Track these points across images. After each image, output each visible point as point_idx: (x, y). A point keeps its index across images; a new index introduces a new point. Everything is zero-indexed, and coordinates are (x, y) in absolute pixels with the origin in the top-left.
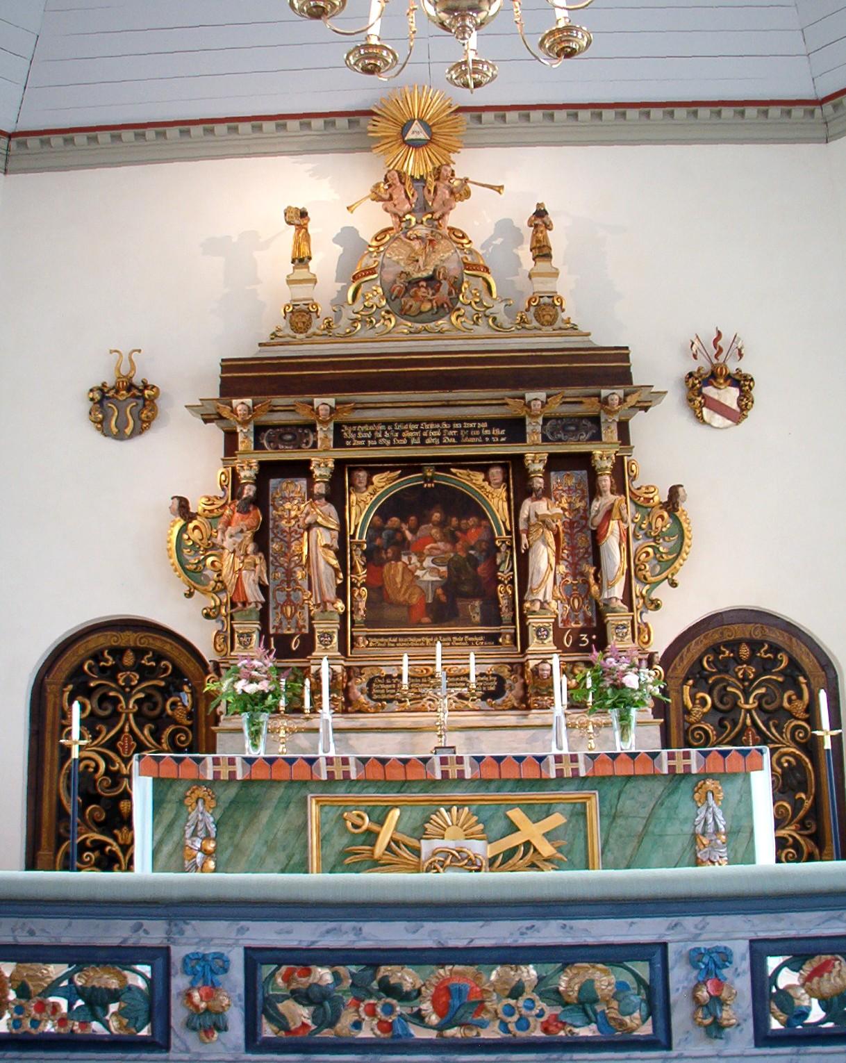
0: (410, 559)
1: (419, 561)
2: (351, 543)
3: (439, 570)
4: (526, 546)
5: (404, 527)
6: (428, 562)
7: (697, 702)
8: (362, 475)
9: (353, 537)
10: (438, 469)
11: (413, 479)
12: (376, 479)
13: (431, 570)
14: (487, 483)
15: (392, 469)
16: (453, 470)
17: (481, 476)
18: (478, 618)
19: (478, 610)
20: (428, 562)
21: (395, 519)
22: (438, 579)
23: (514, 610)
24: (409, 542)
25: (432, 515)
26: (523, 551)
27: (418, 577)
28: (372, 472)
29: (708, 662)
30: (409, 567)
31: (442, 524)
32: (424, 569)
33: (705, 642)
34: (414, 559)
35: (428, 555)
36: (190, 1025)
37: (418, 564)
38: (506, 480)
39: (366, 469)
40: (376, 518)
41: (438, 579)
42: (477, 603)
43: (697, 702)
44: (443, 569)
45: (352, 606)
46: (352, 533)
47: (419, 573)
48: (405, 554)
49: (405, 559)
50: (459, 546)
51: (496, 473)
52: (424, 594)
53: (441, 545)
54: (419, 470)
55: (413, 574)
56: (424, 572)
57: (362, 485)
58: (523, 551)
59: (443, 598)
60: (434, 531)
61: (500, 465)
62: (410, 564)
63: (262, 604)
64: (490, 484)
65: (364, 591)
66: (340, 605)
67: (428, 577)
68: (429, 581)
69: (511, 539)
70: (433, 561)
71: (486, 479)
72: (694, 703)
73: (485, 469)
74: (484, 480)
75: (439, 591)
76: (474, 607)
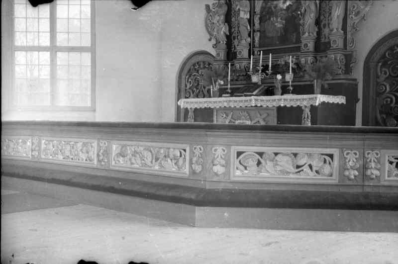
0: (273, 19)
6: (279, 20)
7: (383, 72)
18: (294, 41)
19: (295, 37)
20: (279, 20)
22: (282, 26)
29: (388, 54)
32: (277, 22)
33: (388, 45)
34: (275, 19)
36: (379, 183)
43: (383, 72)
44: (284, 22)
47: (276, 24)
49: (272, 19)
52: (277, 32)
65: (258, 34)
66: (249, 39)
70: (281, 19)
72: (381, 73)
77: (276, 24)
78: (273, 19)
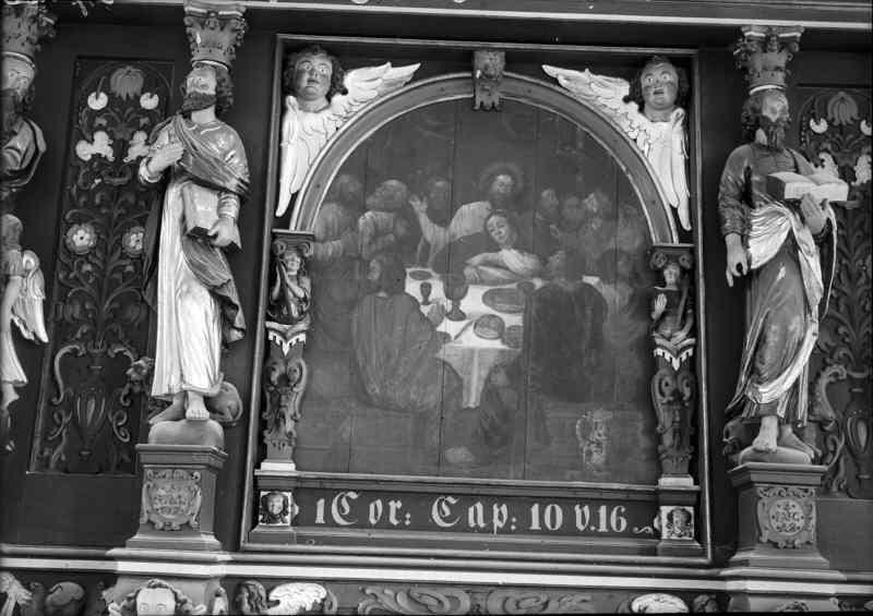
0: (426, 289)
1: (448, 296)
2: (274, 236)
3: (501, 324)
4: (739, 267)
5: (419, 206)
8: (319, 67)
9: (284, 221)
10: (513, 61)
11: (448, 89)
12: (353, 79)
13: (481, 324)
14: (634, 106)
15: (399, 58)
16: (548, 69)
17: (624, 88)
18: (598, 458)
19: (599, 434)
21: (394, 183)
23: (695, 441)
24: (428, 245)
25: (492, 177)
26: (731, 283)
27: (446, 337)
28: (348, 59)
30: (425, 310)
31: (514, 205)
32: (461, 316)
34: (438, 290)
35: (475, 282)
37: (448, 305)
38: (684, 100)
39: (331, 51)
40: (345, 179)
41: (498, 345)
42: (598, 416)
44: (513, 320)
45: (262, 407)
46: (280, 212)
47: (449, 326)
48: (414, 275)
49: (413, 288)
50: (556, 260)
51: (661, 79)
53: (512, 258)
54: (465, 61)
55: (433, 327)
56: (463, 324)
57: (320, 89)
58: (731, 283)
59: (507, 396)
60: (494, 220)
61: (675, 61)
62: (426, 302)
63: (17, 390)
64: (641, 110)
67: (472, 340)
68: (472, 351)
69: (693, 251)
70: (488, 298)
71: (637, 97)
73: (630, 69)
74: (627, 100)
75: (501, 379)
76: (588, 428)
77: (449, 326)
78: (426, 289)
